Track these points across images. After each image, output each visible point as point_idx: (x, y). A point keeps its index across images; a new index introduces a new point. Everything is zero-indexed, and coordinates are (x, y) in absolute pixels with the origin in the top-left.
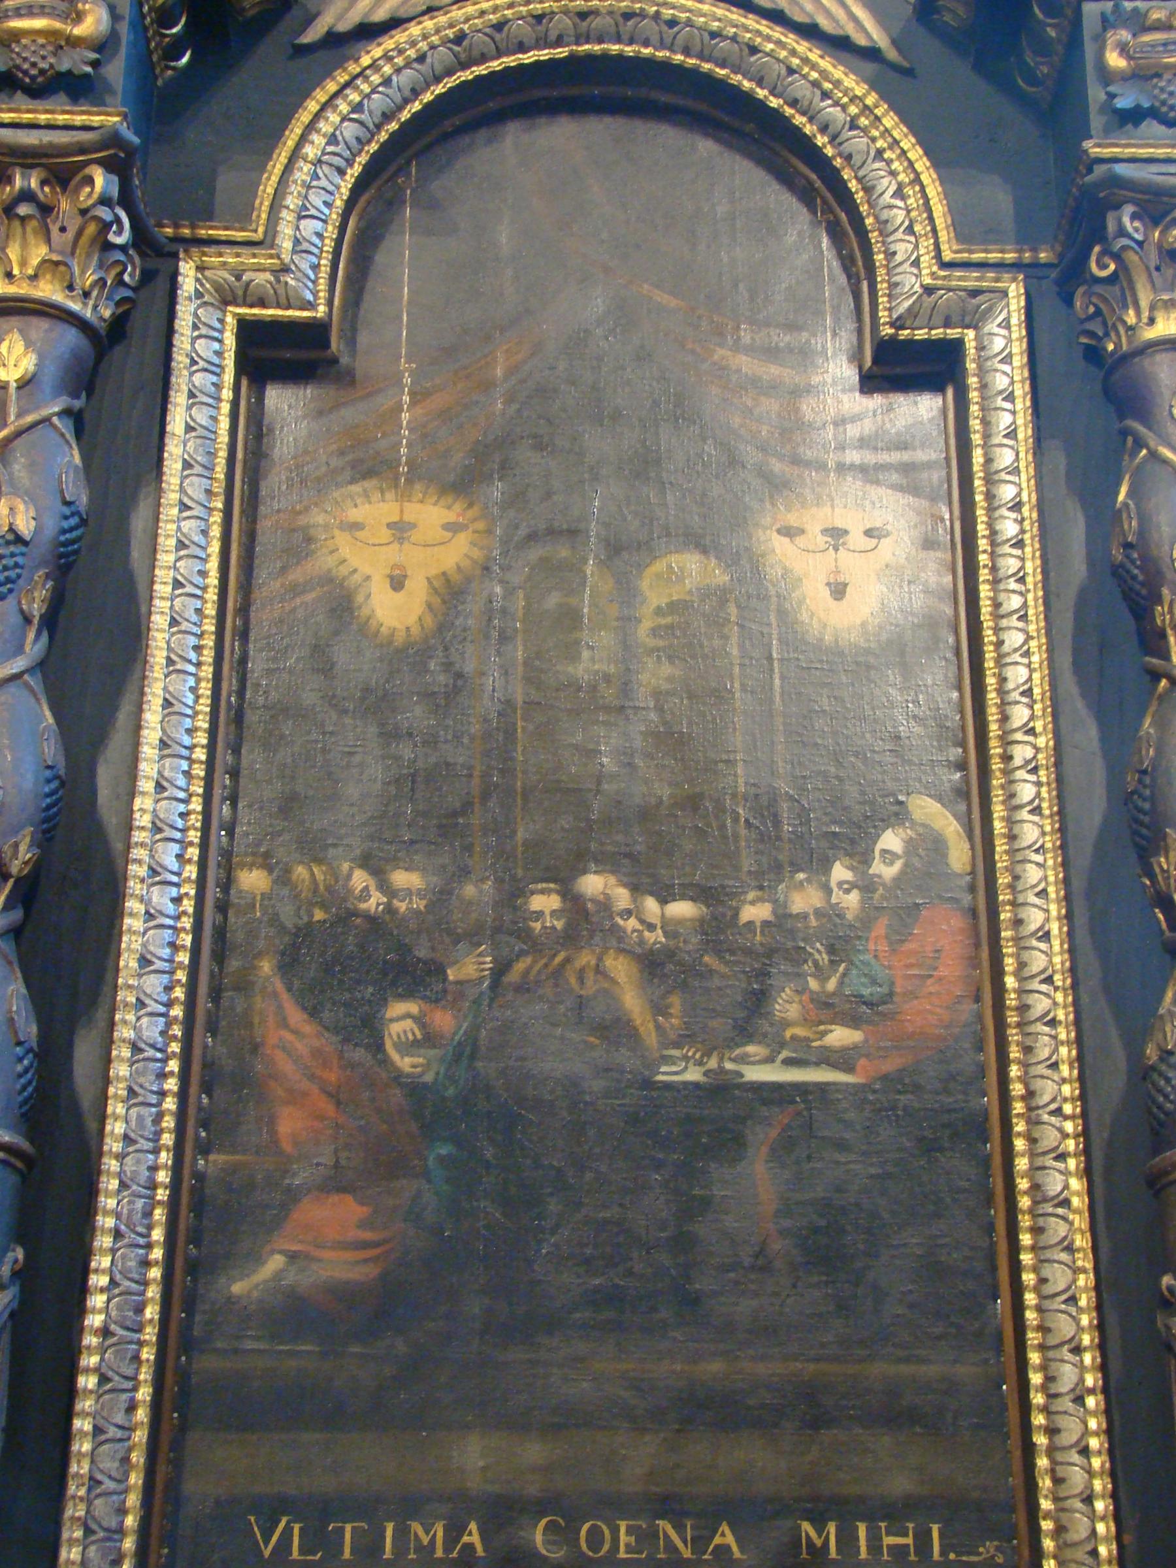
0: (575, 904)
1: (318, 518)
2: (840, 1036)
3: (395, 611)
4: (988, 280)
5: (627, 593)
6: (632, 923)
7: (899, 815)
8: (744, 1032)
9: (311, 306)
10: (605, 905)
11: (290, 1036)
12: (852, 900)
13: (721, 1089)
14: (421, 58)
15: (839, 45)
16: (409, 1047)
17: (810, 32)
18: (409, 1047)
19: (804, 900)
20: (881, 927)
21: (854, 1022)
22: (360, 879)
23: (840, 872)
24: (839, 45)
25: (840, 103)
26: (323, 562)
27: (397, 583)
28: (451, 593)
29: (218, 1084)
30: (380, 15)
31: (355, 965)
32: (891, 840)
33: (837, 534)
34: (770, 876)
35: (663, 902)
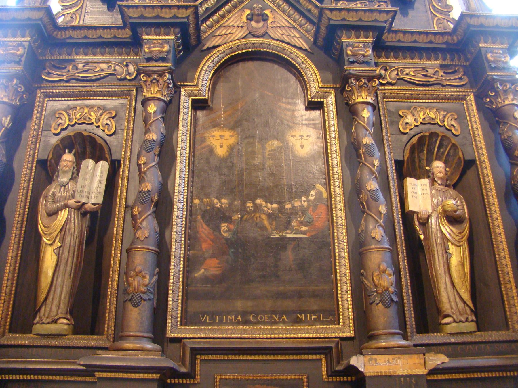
0: (255, 205)
1: (207, 135)
2: (304, 228)
3: (221, 152)
4: (328, 90)
5: (264, 148)
6: (266, 208)
7: (314, 188)
8: (287, 228)
9: (205, 96)
10: (261, 205)
11: (204, 230)
12: (306, 204)
13: (283, 238)
14: (224, 52)
15: (300, 49)
16: (225, 232)
17: (294, 46)
18: (225, 232)
19: (297, 204)
20: (311, 208)
21: (306, 226)
22: (216, 201)
23: (303, 199)
24: (300, 49)
25: (300, 59)
26: (208, 143)
27: (221, 146)
28: (231, 148)
29: (191, 239)
30: (217, 44)
32: (313, 193)
33: (302, 136)
35: (271, 204)
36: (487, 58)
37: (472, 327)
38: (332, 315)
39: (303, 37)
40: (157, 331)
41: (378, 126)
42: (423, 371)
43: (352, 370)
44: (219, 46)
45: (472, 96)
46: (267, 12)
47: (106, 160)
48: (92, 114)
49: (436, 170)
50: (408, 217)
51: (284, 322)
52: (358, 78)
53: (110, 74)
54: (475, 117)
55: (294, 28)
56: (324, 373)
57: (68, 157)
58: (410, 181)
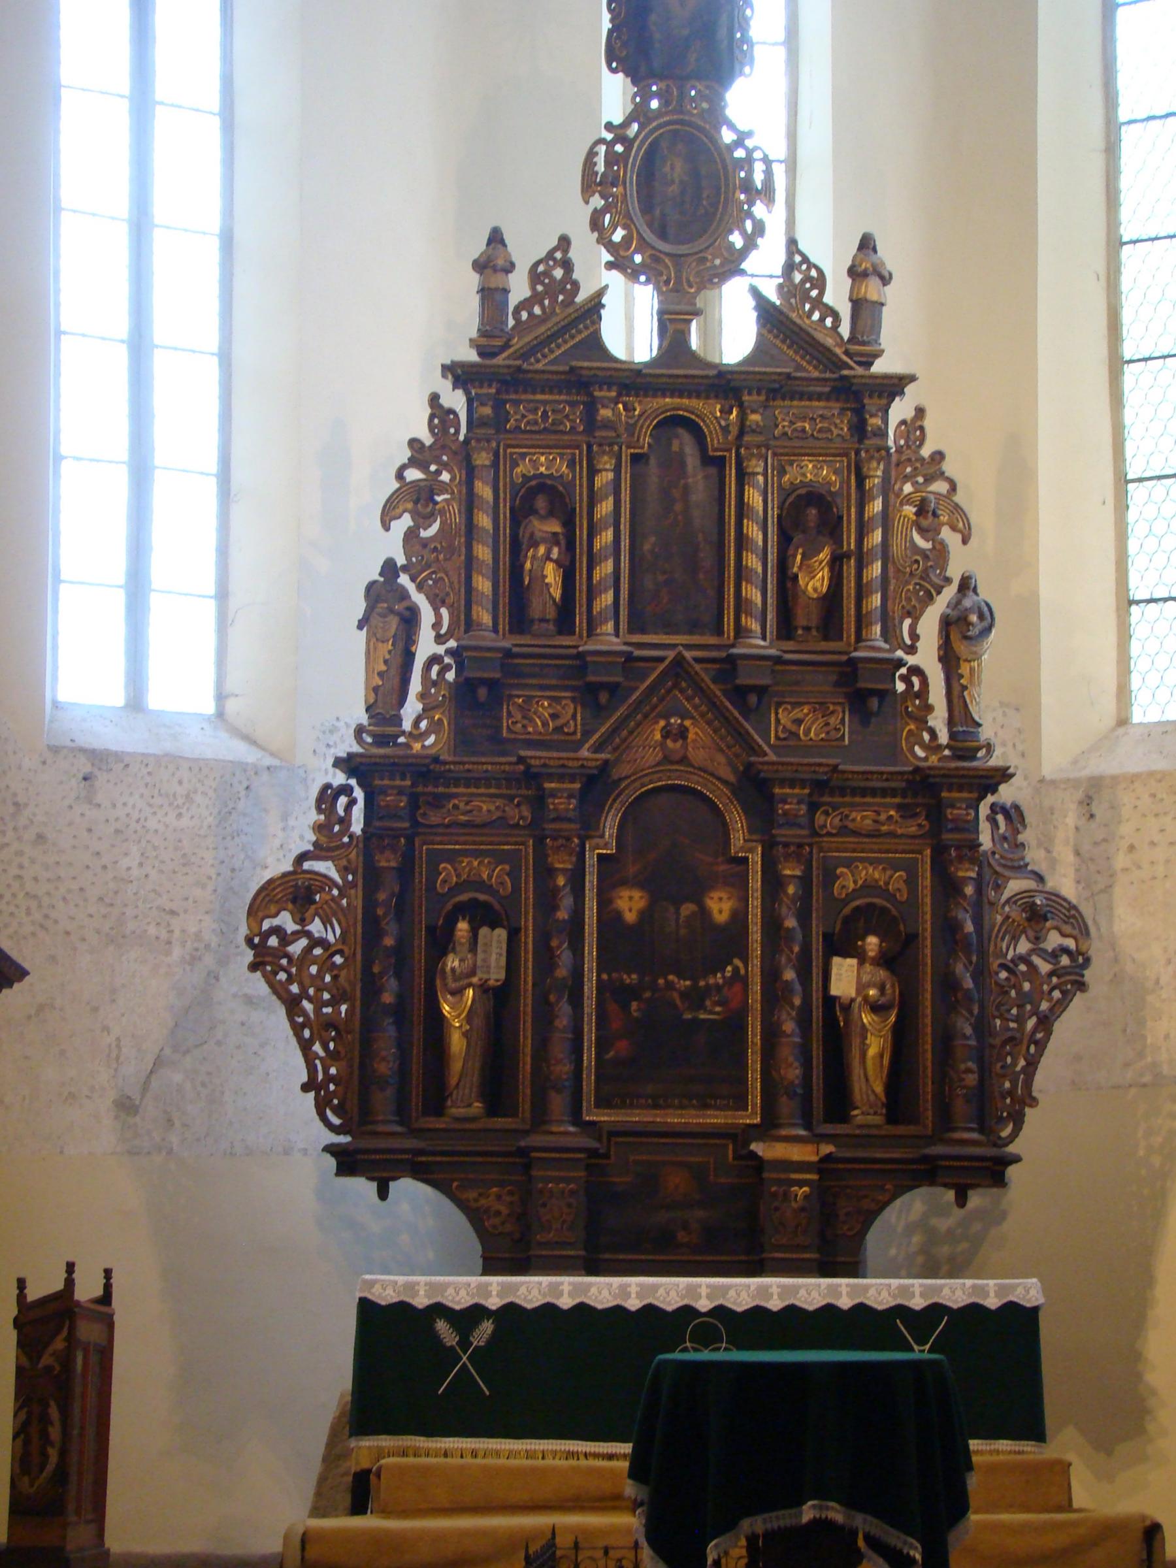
0: (666, 981)
3: (630, 917)
5: (677, 913)
7: (731, 963)
10: (673, 982)
11: (612, 1007)
12: (721, 981)
17: (719, 779)
21: (720, 1005)
22: (625, 976)
23: (719, 975)
26: (614, 906)
27: (630, 910)
28: (642, 914)
32: (729, 968)
34: (705, 977)
36: (946, 816)
37: (878, 1120)
38: (740, 1102)
39: (730, 763)
40: (576, 1116)
41: (805, 896)
42: (815, 1158)
43: (753, 1155)
44: (627, 777)
45: (929, 851)
46: (687, 723)
47: (504, 927)
48: (483, 869)
49: (868, 948)
50: (830, 1001)
51: (694, 1107)
52: (786, 845)
53: (499, 818)
54: (926, 880)
55: (722, 751)
56: (731, 1156)
57: (463, 926)
58: (836, 960)
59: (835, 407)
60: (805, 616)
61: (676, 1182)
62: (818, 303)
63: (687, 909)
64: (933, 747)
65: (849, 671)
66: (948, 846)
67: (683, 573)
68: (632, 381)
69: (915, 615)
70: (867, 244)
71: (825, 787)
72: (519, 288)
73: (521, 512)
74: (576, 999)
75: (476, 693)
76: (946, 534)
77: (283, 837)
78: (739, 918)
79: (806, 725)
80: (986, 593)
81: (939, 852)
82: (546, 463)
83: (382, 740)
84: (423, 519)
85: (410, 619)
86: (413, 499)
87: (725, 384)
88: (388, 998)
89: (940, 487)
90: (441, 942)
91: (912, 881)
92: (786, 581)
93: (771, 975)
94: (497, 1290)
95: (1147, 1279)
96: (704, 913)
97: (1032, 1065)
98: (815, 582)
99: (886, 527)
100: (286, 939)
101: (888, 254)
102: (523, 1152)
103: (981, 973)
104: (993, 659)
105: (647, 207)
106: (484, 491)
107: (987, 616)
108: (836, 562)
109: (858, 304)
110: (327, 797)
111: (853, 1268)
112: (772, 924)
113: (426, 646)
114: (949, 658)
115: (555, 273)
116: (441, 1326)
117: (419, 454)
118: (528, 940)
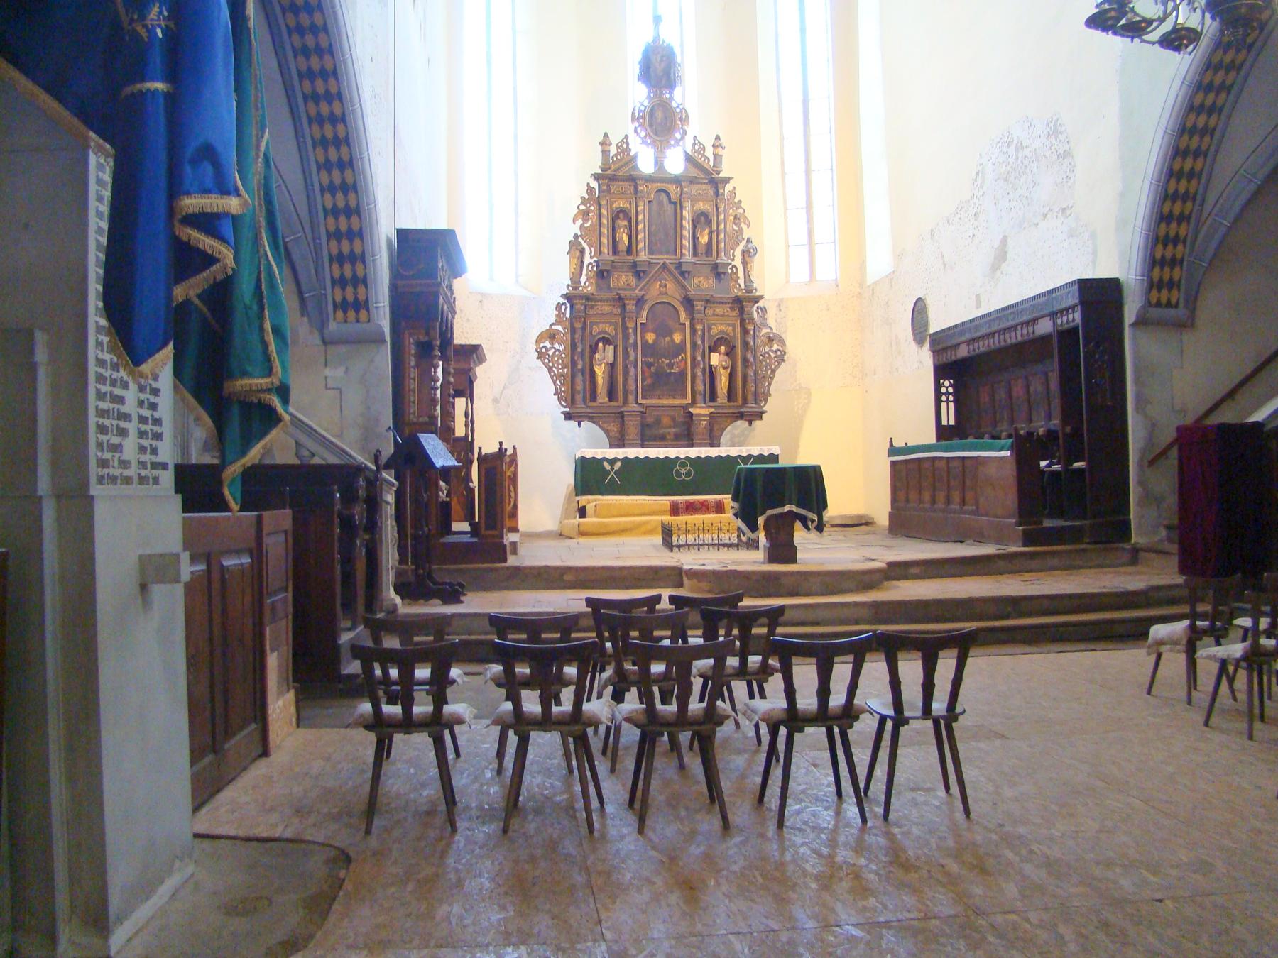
3: (650, 342)
29: (643, 372)
31: (649, 365)
38: (684, 396)
50: (710, 366)
54: (738, 329)
57: (601, 345)
59: (708, 187)
60: (701, 250)
61: (666, 421)
62: (703, 155)
63: (668, 339)
64: (740, 289)
65: (716, 266)
66: (744, 320)
67: (666, 237)
68: (649, 179)
69: (734, 249)
70: (717, 138)
71: (708, 302)
72: (613, 150)
73: (615, 218)
74: (636, 367)
75: (602, 274)
76: (743, 225)
77: (545, 317)
78: (684, 341)
79: (702, 284)
80: (754, 243)
81: (742, 321)
82: (622, 204)
83: (575, 289)
84: (585, 221)
85: (582, 252)
86: (585, 215)
87: (676, 180)
88: (580, 367)
89: (741, 211)
90: (594, 350)
91: (734, 330)
92: (695, 238)
93: (693, 359)
94: (620, 453)
95: (797, 446)
96: (673, 340)
97: (770, 384)
98: (704, 239)
99: (726, 226)
100: (547, 350)
101: (723, 141)
102: (621, 413)
103: (755, 358)
104: (756, 263)
105: (651, 125)
106: (604, 212)
107: (755, 249)
108: (710, 233)
109: (715, 156)
110: (559, 306)
111: (718, 445)
112: (694, 344)
113: (587, 260)
114: (744, 263)
115: (624, 147)
116: (605, 464)
117: (584, 201)
118: (620, 349)
